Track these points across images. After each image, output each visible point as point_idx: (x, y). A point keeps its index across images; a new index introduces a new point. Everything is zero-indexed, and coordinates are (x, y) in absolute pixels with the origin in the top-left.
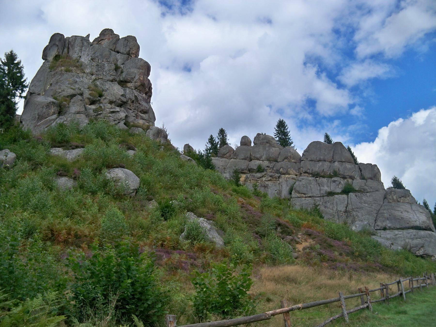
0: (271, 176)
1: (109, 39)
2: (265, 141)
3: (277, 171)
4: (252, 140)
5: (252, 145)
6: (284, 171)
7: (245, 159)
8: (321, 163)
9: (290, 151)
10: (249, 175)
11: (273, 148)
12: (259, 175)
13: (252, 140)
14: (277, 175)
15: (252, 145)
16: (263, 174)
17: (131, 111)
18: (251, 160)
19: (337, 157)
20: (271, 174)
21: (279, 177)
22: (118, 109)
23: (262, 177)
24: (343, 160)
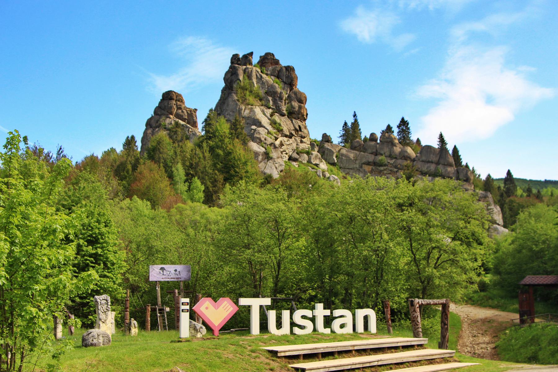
0: (391, 170)
1: (271, 64)
2: (389, 140)
3: (396, 167)
4: (379, 135)
5: (379, 141)
6: (401, 168)
7: (372, 153)
8: (429, 164)
9: (407, 152)
10: (374, 168)
11: (395, 148)
12: (382, 168)
13: (379, 138)
14: (395, 170)
15: (379, 141)
16: (385, 168)
17: (297, 138)
18: (376, 155)
19: (442, 161)
20: (390, 169)
21: (397, 172)
22: (291, 141)
23: (385, 170)
24: (446, 164)
